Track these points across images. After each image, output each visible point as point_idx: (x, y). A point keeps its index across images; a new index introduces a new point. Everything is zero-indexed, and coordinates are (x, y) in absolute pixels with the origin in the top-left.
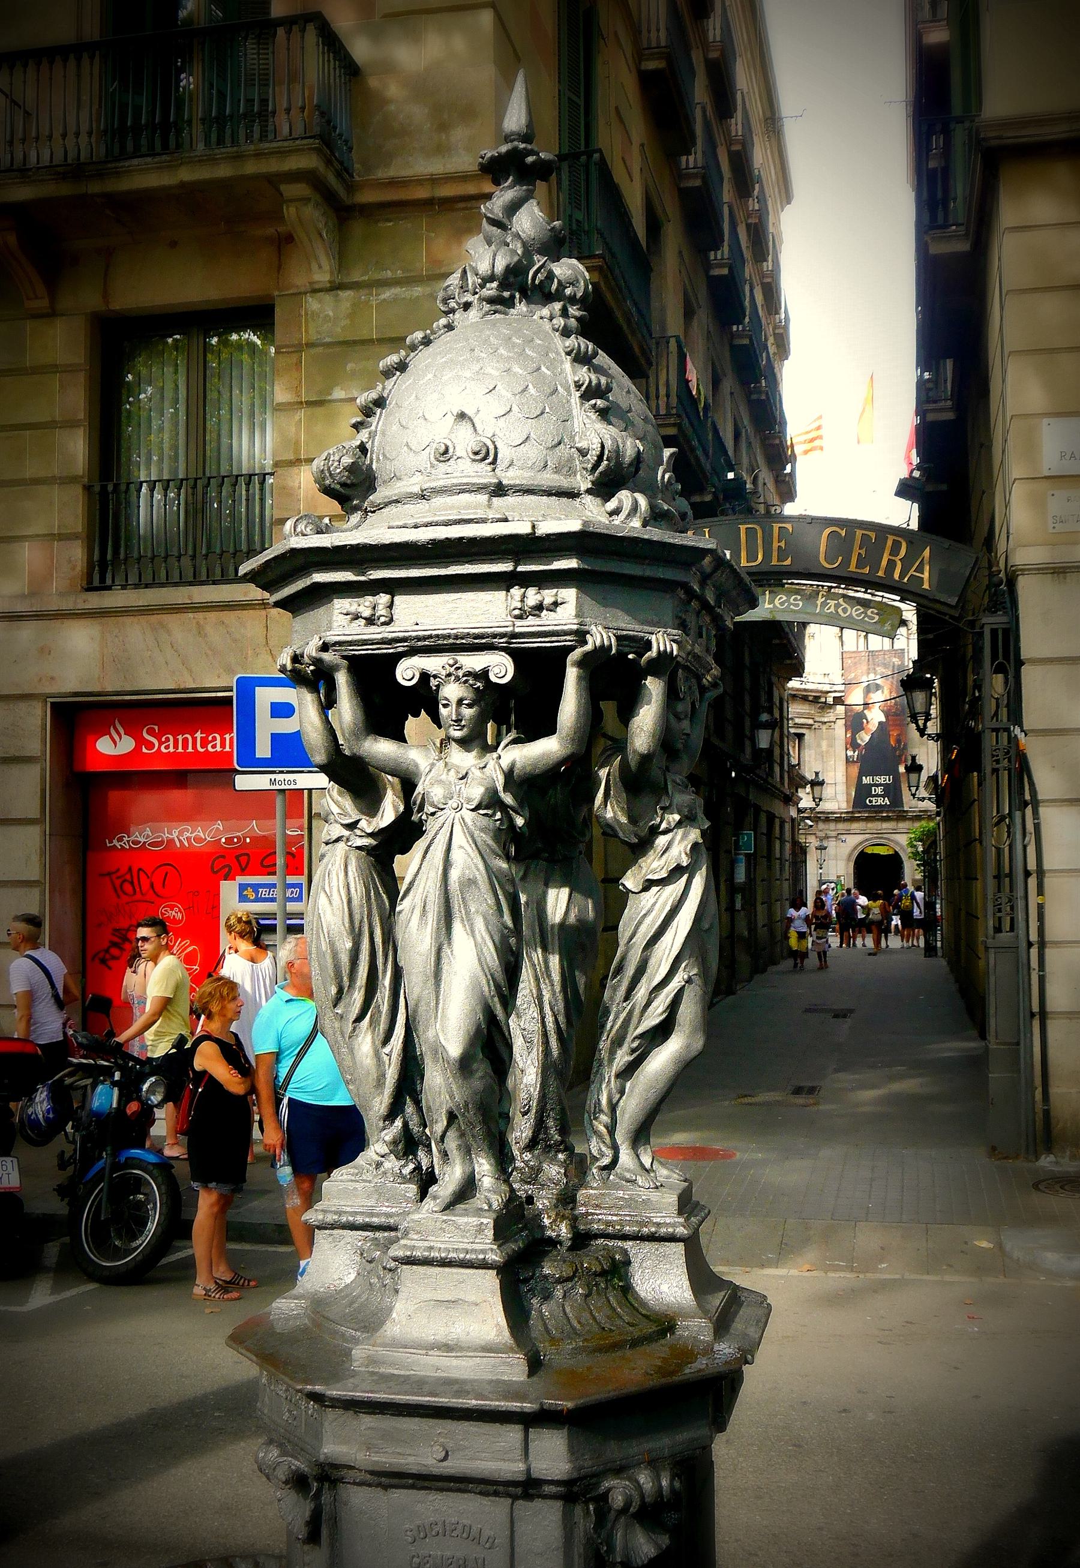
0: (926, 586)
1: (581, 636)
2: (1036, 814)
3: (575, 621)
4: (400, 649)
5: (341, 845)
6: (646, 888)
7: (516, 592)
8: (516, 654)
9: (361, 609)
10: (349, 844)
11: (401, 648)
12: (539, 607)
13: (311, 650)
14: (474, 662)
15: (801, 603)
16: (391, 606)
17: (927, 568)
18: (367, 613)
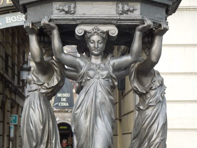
1: (143, 22)
3: (141, 16)
4: (78, 23)
5: (37, 92)
6: (147, 108)
7: (120, 6)
8: (118, 27)
9: (64, 8)
10: (40, 91)
11: (78, 22)
12: (128, 10)
13: (45, 21)
14: (104, 28)
16: (75, 7)
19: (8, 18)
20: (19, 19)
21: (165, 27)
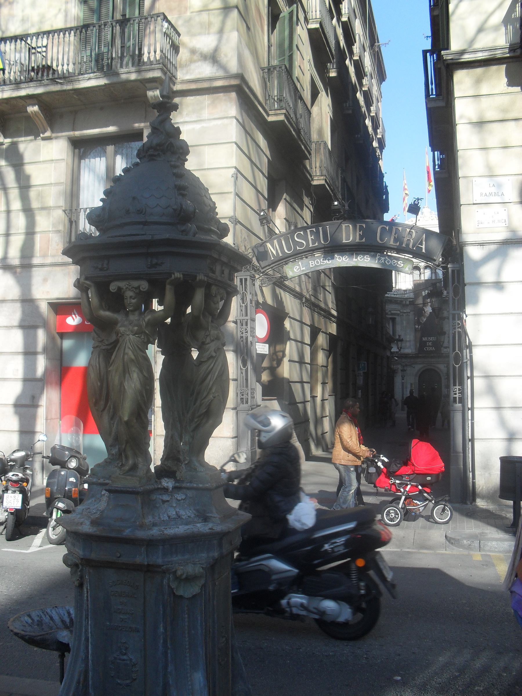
0: (424, 251)
2: (471, 352)
12: (156, 264)
15: (369, 259)
17: (424, 243)
18: (100, 266)
19: (312, 262)
20: (322, 262)
21: (200, 278)
